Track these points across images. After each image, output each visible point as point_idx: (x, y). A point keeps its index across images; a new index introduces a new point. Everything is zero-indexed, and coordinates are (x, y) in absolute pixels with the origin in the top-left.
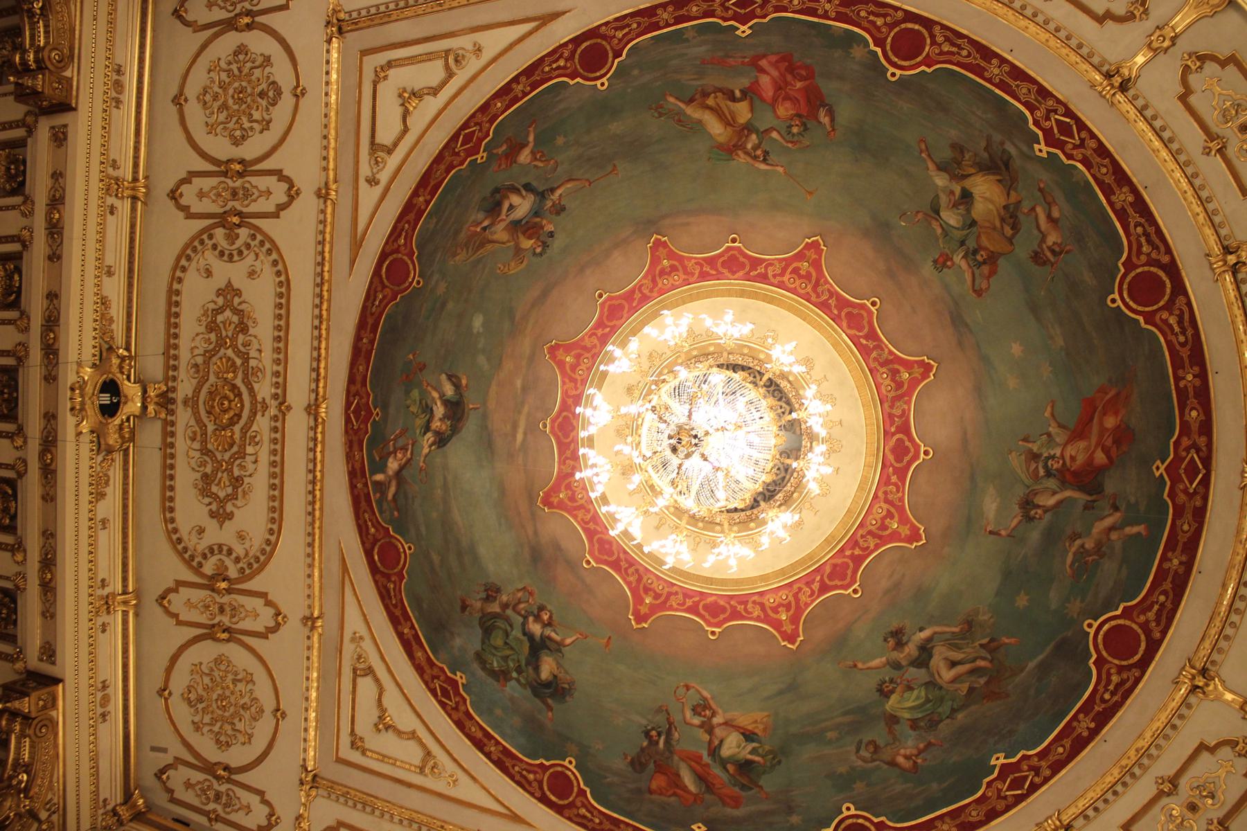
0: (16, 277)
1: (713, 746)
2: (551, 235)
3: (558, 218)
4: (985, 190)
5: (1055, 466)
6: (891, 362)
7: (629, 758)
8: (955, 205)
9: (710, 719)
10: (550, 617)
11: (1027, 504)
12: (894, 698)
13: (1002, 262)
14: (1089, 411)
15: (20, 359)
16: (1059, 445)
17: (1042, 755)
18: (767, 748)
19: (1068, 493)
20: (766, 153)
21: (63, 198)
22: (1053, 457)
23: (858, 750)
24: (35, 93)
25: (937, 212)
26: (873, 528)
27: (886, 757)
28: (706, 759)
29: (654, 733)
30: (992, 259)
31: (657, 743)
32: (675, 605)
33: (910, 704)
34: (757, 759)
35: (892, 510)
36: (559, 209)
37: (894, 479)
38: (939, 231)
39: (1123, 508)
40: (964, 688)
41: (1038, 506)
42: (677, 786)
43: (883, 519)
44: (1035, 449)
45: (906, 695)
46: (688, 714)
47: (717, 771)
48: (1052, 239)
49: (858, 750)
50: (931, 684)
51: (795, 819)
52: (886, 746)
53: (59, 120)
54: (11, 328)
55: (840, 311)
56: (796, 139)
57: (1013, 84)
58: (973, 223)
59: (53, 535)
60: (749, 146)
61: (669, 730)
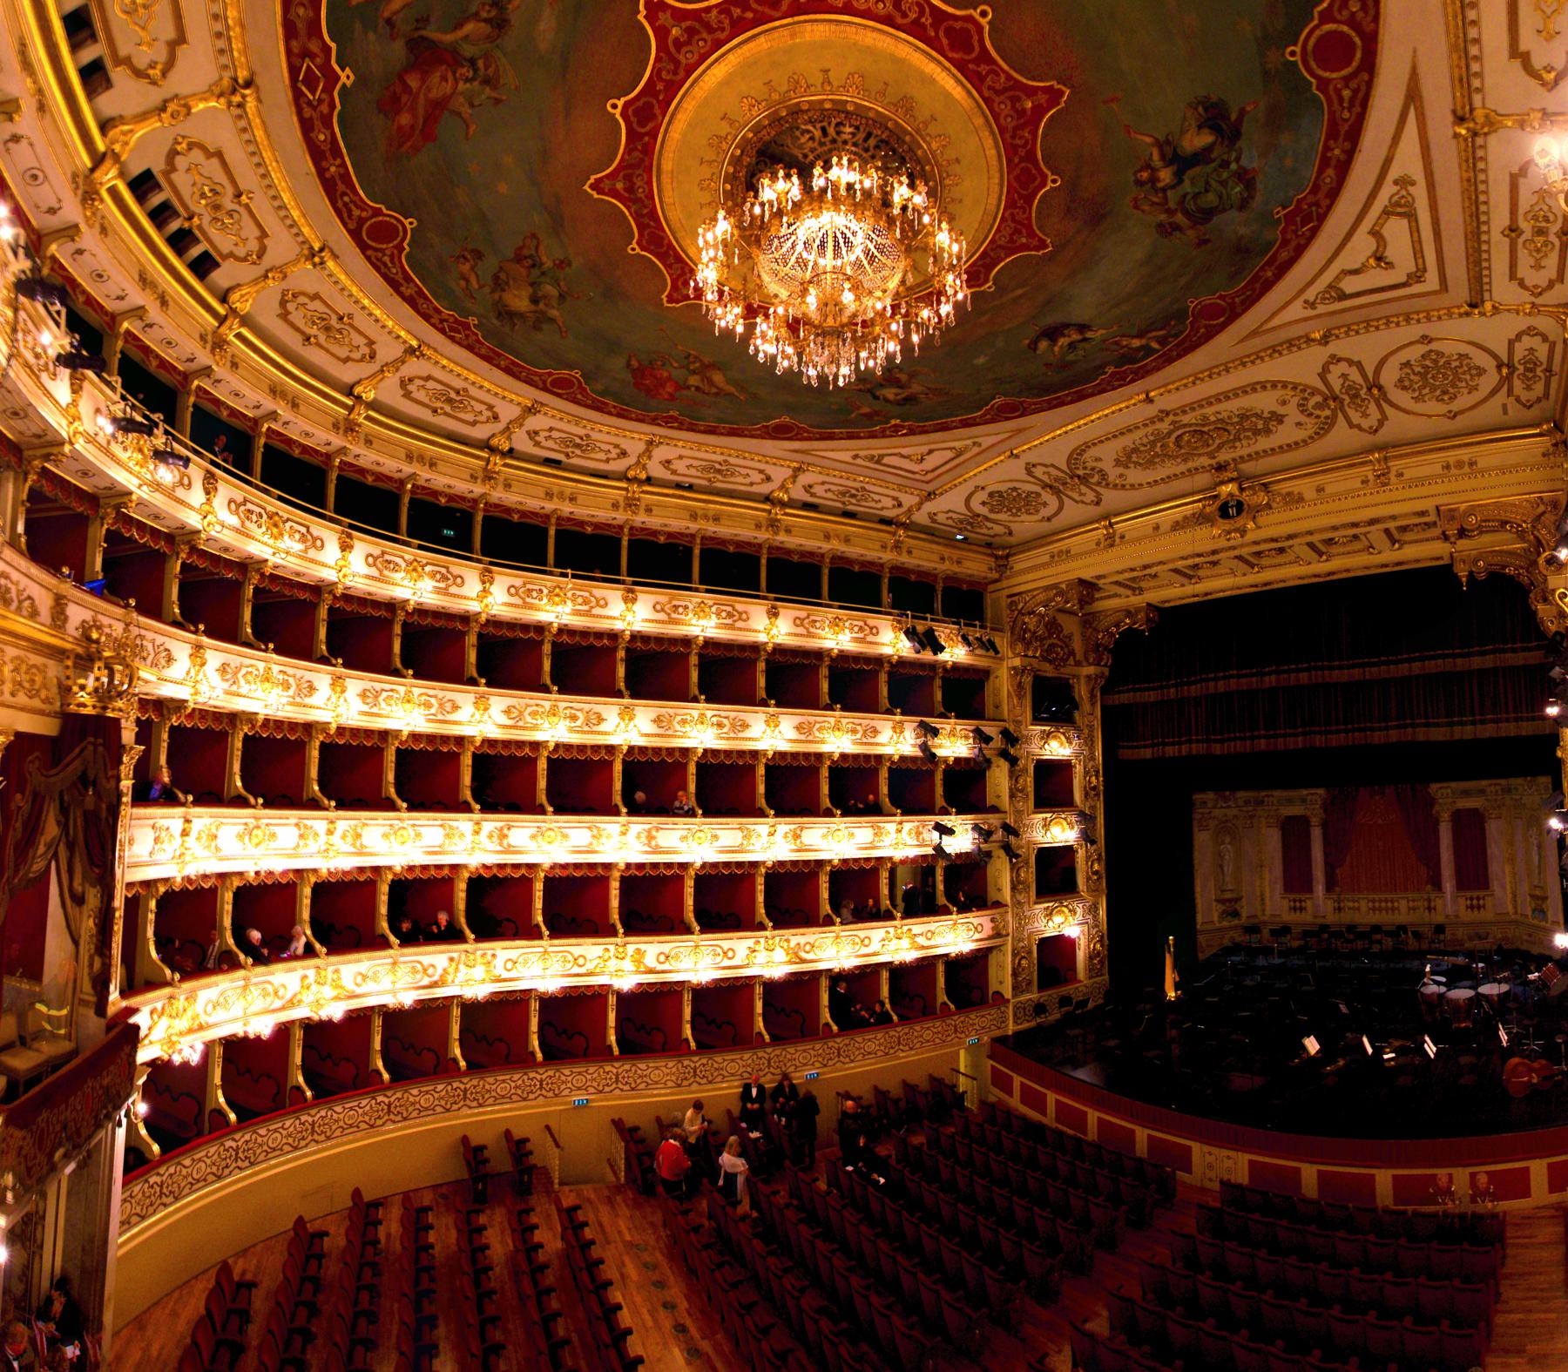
4: (519, 300)
5: (465, 70)
6: (630, 200)
8: (545, 297)
13: (510, 254)
16: (462, 94)
19: (448, 38)
22: (467, 80)
25: (560, 295)
26: (705, 35)
30: (519, 258)
35: (672, 49)
37: (660, 86)
38: (562, 284)
39: (381, 23)
41: (486, 21)
43: (688, 43)
44: (487, 90)
48: (466, 267)
55: (667, 252)
57: (491, 354)
58: (532, 284)
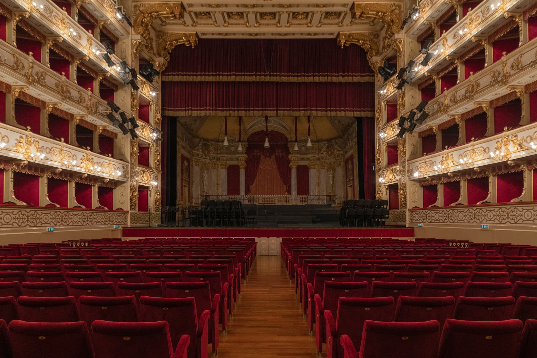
0: (234, 13)
15: (257, 13)
21: (209, 4)
24: (180, 14)
53: (186, 6)
54: (248, 15)
59: (309, 5)
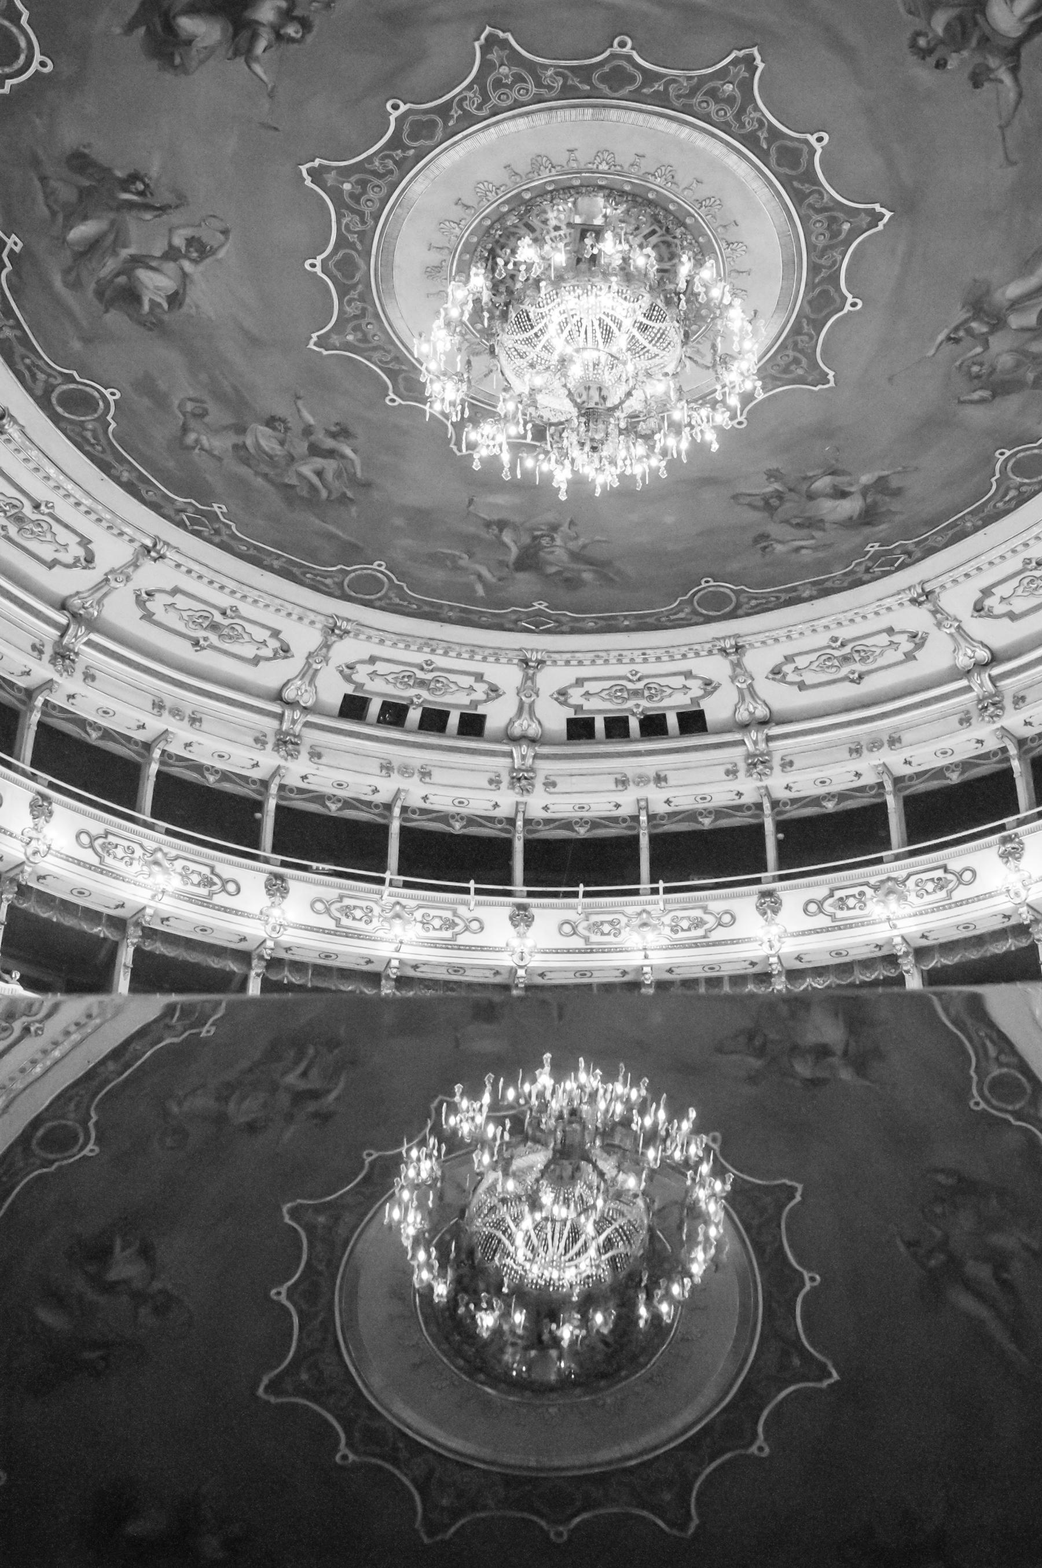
1: (147, 260)
2: (941, 65)
3: (966, 75)
7: (86, 151)
9: (186, 257)
10: (291, 40)
11: (502, 525)
12: (268, 431)
14: (599, 565)
17: (233, 536)
18: (166, 318)
20: (957, 341)
23: (190, 399)
25: (832, 473)
27: (192, 423)
28: (125, 253)
29: (141, 187)
31: (126, 190)
32: (344, 221)
33: (263, 443)
34: (146, 307)
36: (978, 78)
38: (811, 474)
40: (293, 481)
42: (67, 218)
45: (274, 440)
46: (188, 232)
47: (111, 265)
48: (779, 548)
49: (190, 399)
50: (291, 459)
51: (77, 345)
52: (206, 425)
56: (964, 368)
60: (974, 325)
61: (158, 209)
